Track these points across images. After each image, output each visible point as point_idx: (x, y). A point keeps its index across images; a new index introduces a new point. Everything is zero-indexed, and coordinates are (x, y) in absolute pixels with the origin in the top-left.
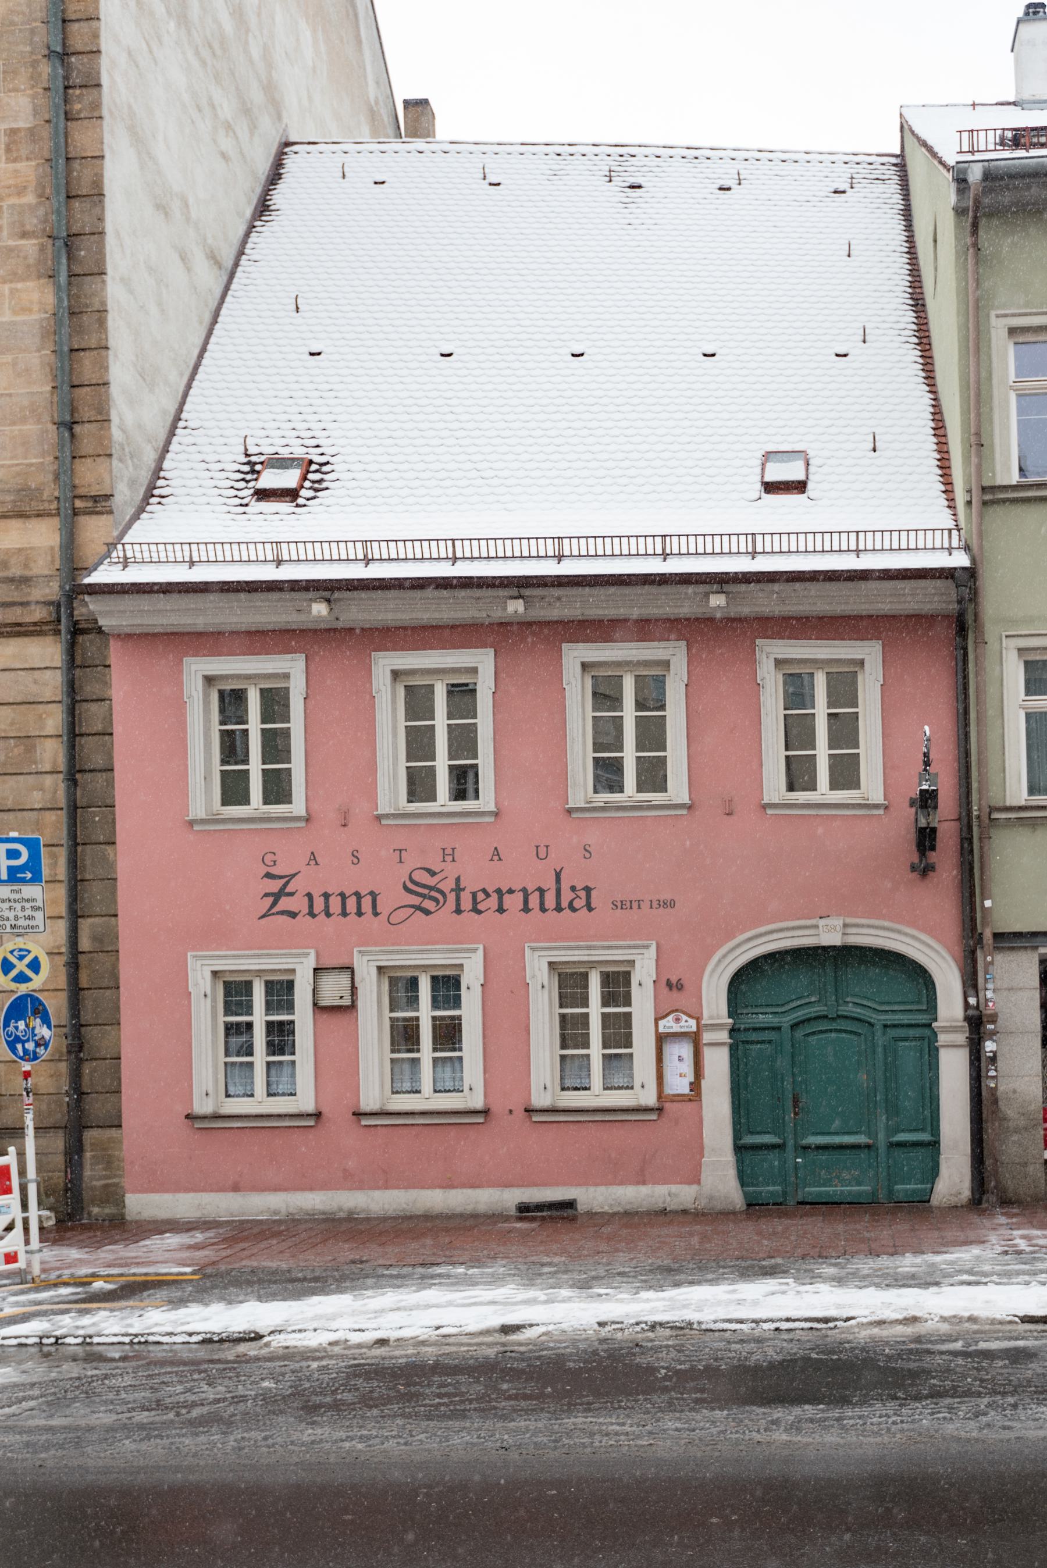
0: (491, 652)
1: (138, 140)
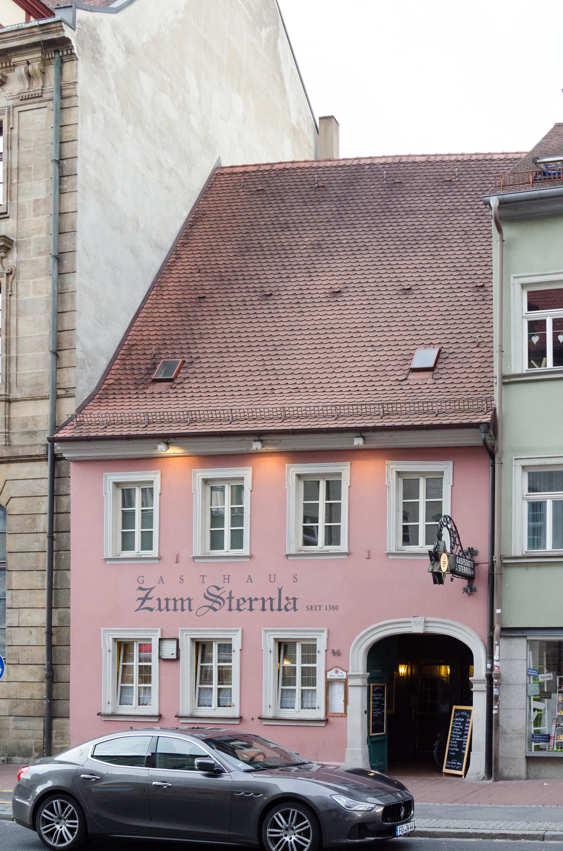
0: (451, 463)
1: (310, 147)
